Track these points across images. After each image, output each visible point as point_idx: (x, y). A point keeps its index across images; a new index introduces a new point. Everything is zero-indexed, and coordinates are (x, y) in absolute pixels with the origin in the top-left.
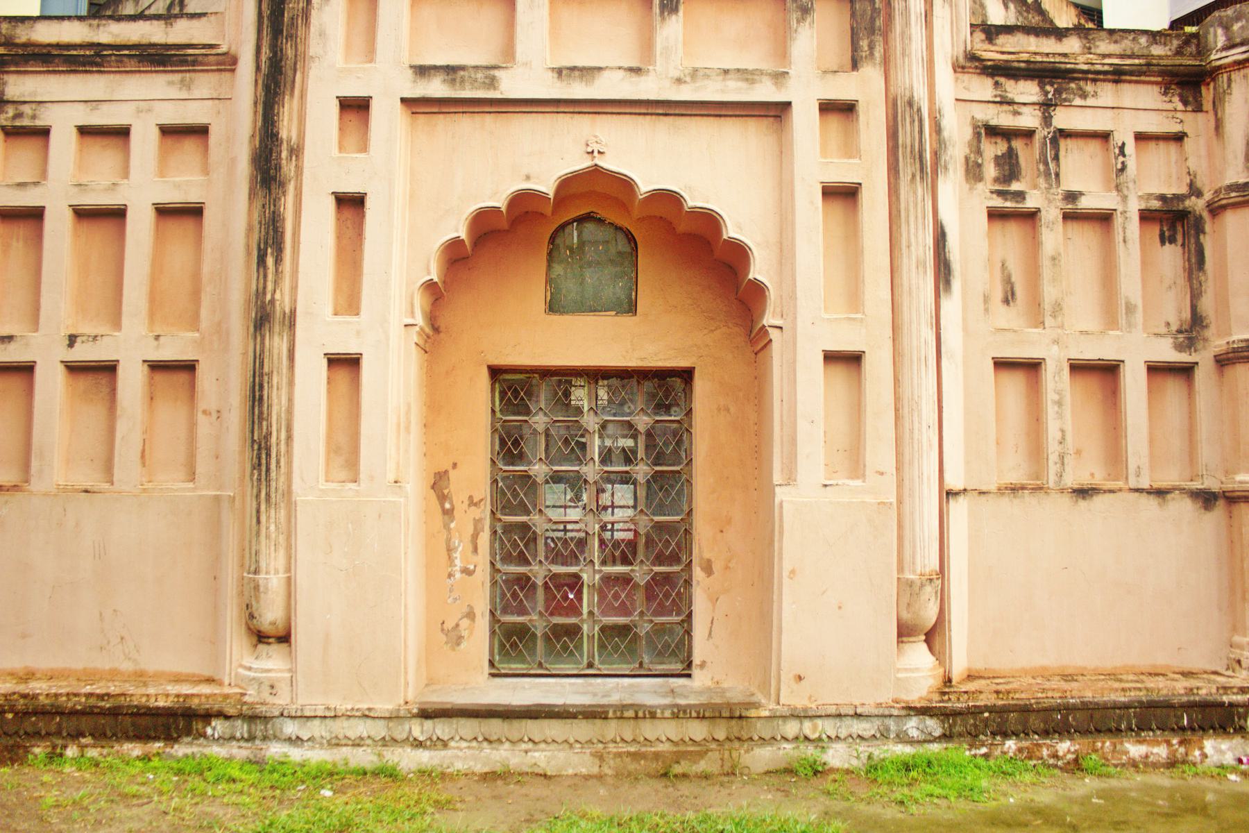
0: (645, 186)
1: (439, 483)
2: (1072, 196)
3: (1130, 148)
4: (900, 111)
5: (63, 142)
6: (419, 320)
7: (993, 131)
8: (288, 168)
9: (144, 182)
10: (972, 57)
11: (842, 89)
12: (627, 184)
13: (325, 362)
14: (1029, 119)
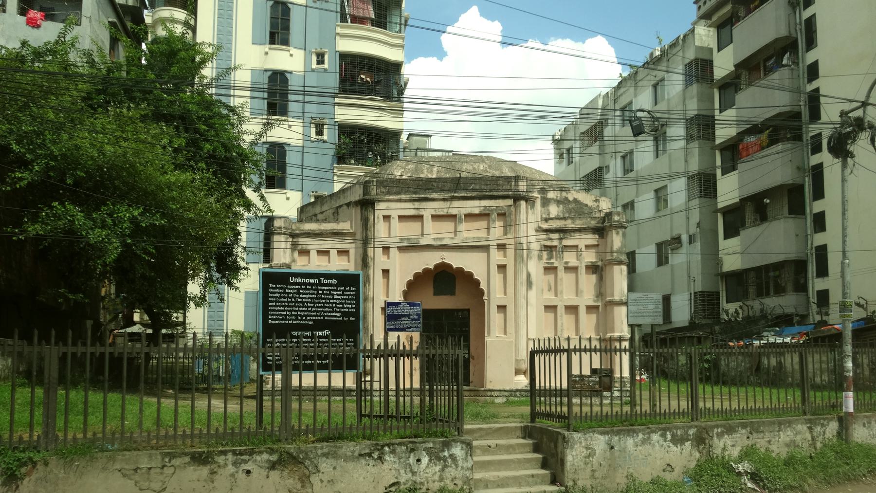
0: (455, 267)
2: (567, 263)
4: (518, 246)
5: (313, 253)
7: (546, 247)
8: (371, 263)
10: (540, 228)
12: (450, 266)
14: (556, 243)
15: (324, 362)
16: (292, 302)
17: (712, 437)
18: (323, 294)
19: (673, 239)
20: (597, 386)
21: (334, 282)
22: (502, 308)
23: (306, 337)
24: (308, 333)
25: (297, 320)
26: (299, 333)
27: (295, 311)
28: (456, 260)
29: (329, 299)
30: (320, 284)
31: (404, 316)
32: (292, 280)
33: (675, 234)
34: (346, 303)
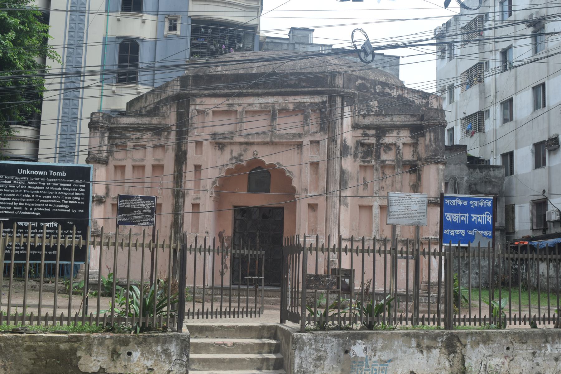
0: (267, 163)
1: (220, 235)
2: (383, 161)
3: (401, 148)
6: (214, 195)
9: (149, 158)
11: (317, 137)
12: (263, 162)
13: (191, 205)
14: (372, 140)
15: (50, 253)
16: (19, 193)
17: (465, 345)
18: (51, 186)
19: (550, 139)
20: (334, 287)
21: (64, 174)
22: (313, 207)
23: (33, 228)
24: (35, 224)
25: (23, 210)
26: (26, 224)
27: (22, 202)
28: (268, 157)
29: (57, 191)
30: (49, 176)
31: (137, 209)
32: (20, 172)
33: (552, 134)
34: (74, 196)
